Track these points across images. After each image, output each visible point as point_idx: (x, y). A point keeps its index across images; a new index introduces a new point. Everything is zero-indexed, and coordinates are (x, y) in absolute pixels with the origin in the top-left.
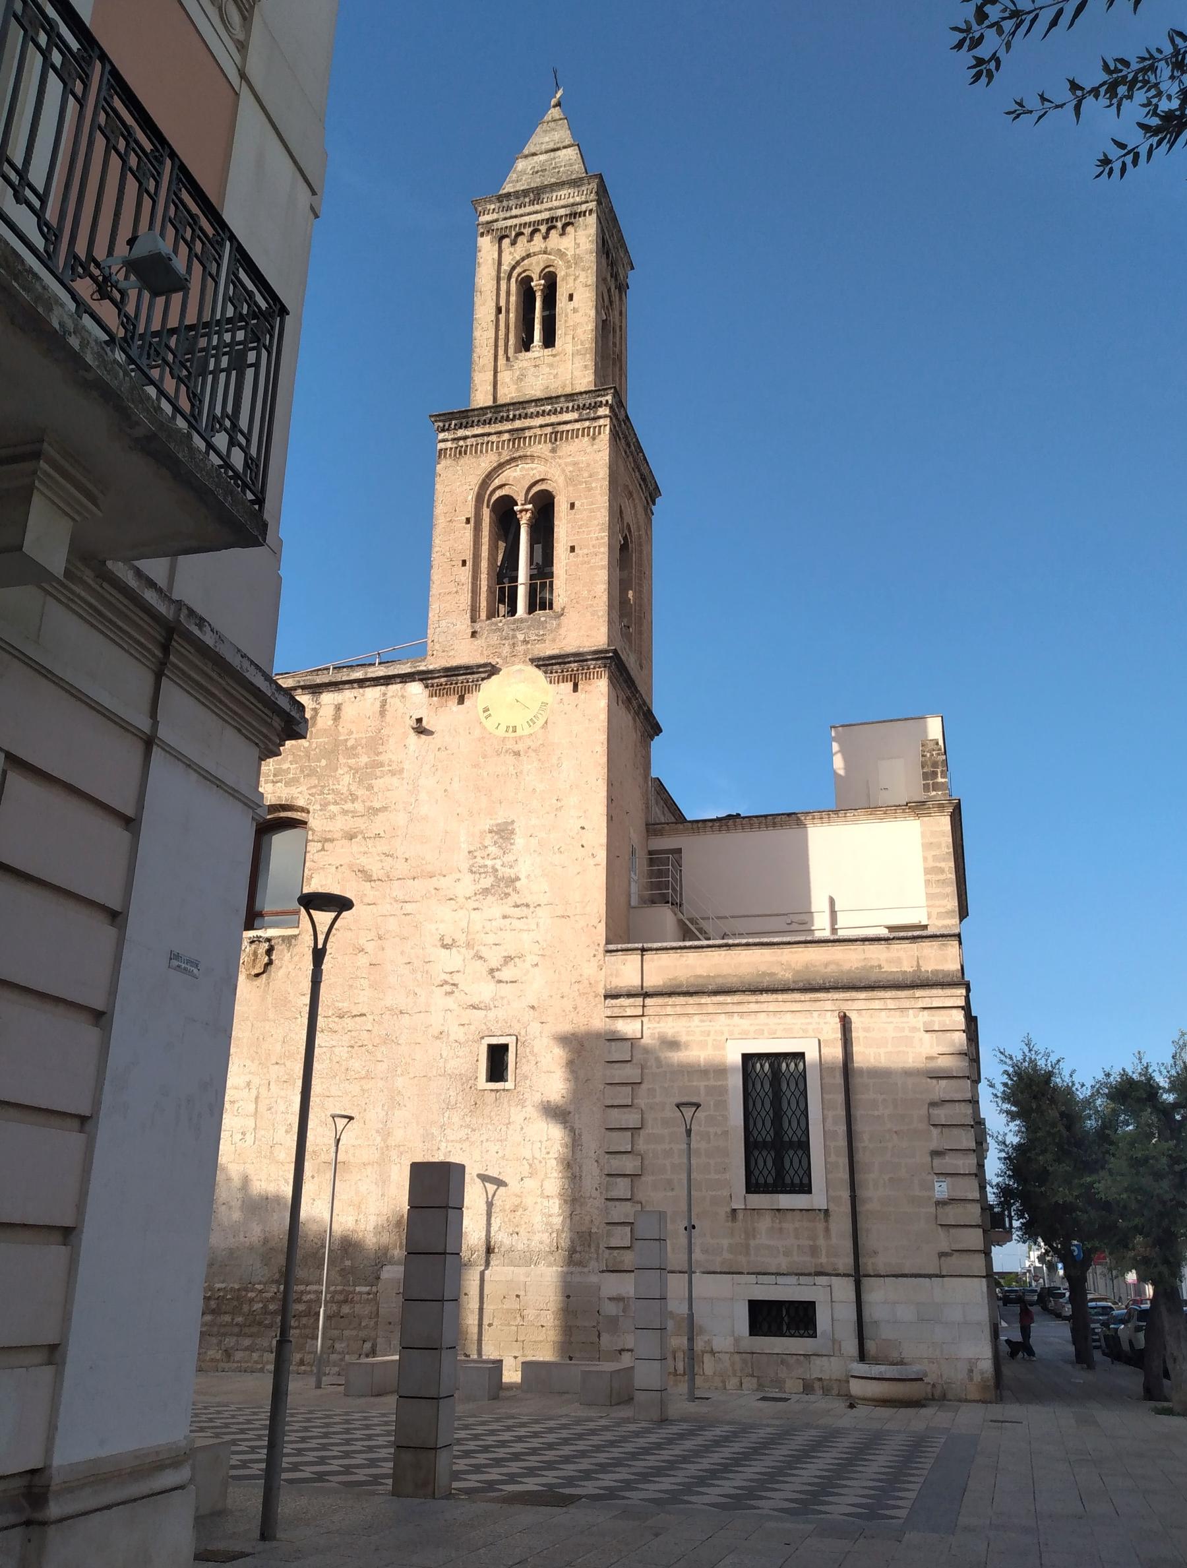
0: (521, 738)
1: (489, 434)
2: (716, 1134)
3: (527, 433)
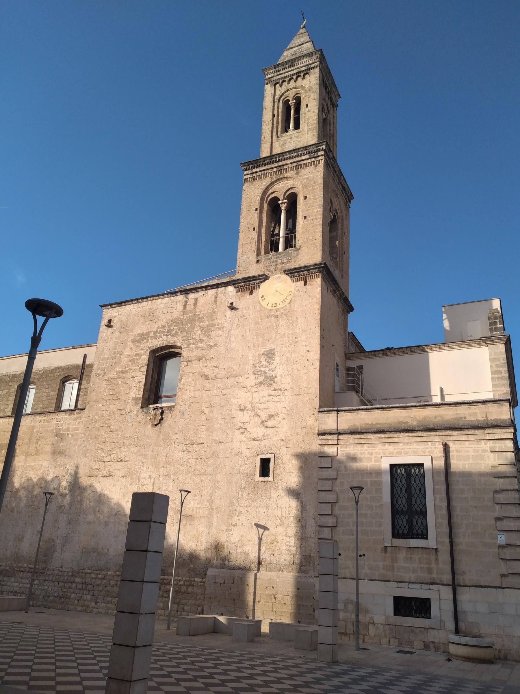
0: (278, 309)
1: (267, 169)
2: (376, 505)
3: (285, 167)
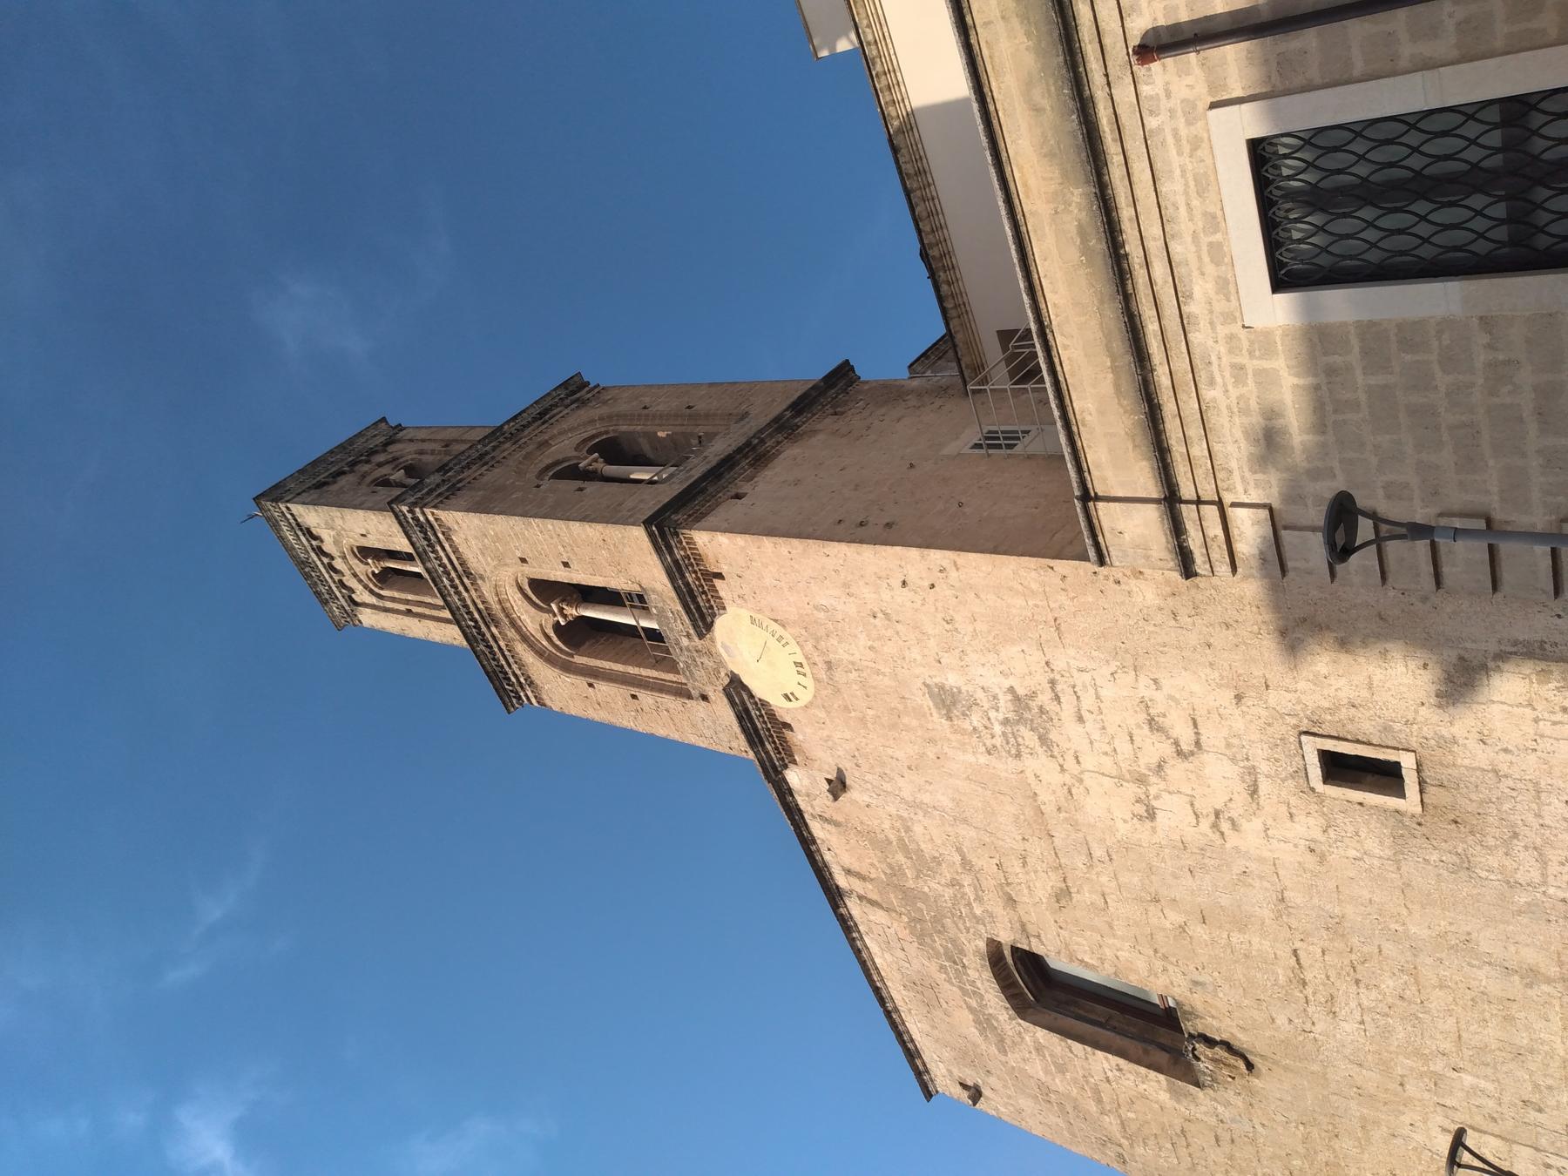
0: (807, 658)
2: (1490, 347)
3: (481, 606)
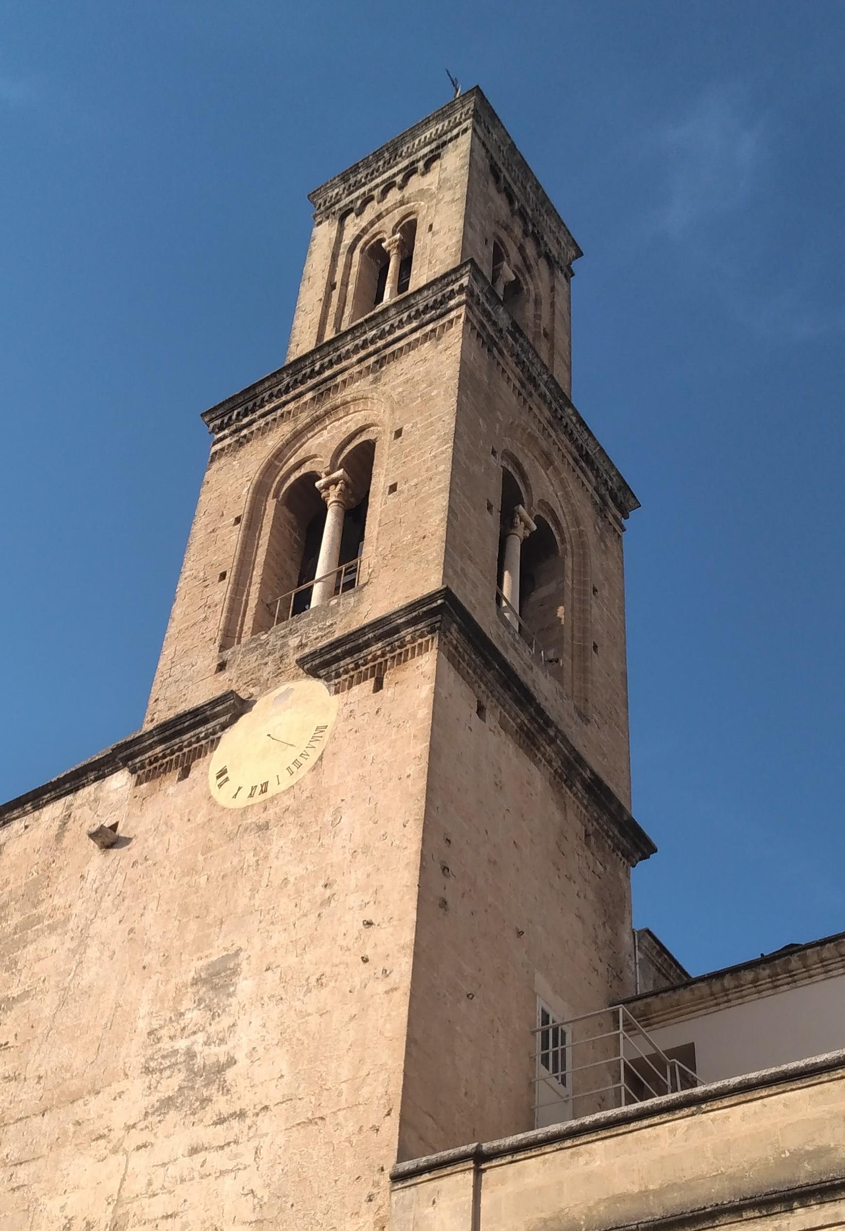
0: (273, 799)
3: (339, 379)
